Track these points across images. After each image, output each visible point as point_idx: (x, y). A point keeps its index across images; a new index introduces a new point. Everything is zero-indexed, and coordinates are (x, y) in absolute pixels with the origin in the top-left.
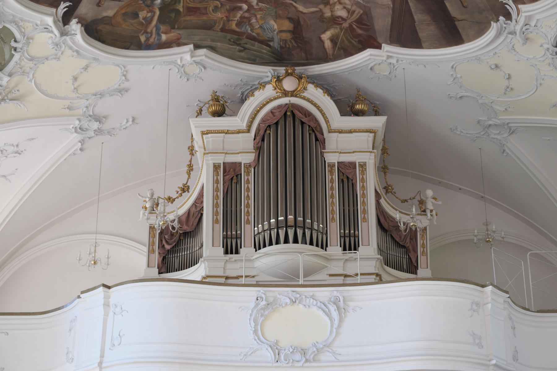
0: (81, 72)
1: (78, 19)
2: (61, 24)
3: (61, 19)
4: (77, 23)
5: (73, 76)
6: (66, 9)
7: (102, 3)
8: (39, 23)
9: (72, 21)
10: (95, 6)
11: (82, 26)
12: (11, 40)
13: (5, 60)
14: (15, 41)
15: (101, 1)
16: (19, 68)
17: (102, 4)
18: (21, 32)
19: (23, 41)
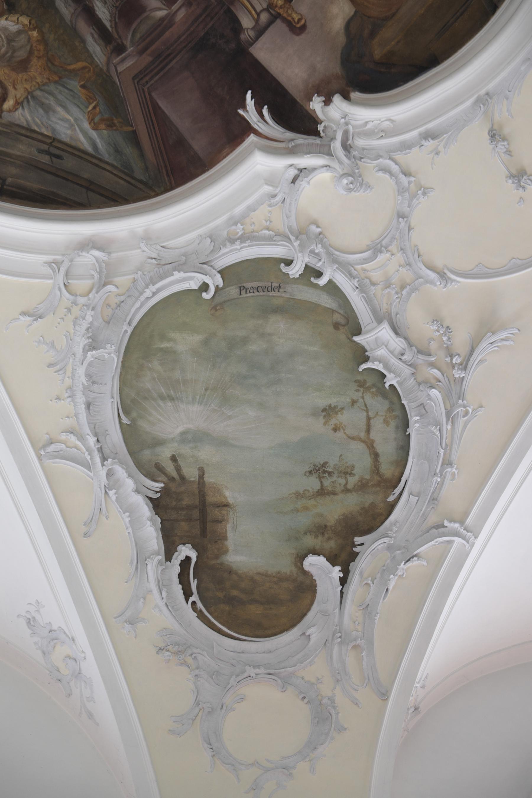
0: (509, 152)
1: (316, 95)
2: (301, 139)
3: (289, 135)
4: (328, 102)
5: (507, 177)
6: (265, 111)
7: (296, 20)
8: (267, 189)
9: (314, 111)
10: (297, 38)
11: (346, 97)
12: (281, 271)
13: (333, 311)
14: (289, 263)
15: (289, 18)
16: (383, 290)
17: (299, 20)
18: (270, 240)
19: (293, 246)
